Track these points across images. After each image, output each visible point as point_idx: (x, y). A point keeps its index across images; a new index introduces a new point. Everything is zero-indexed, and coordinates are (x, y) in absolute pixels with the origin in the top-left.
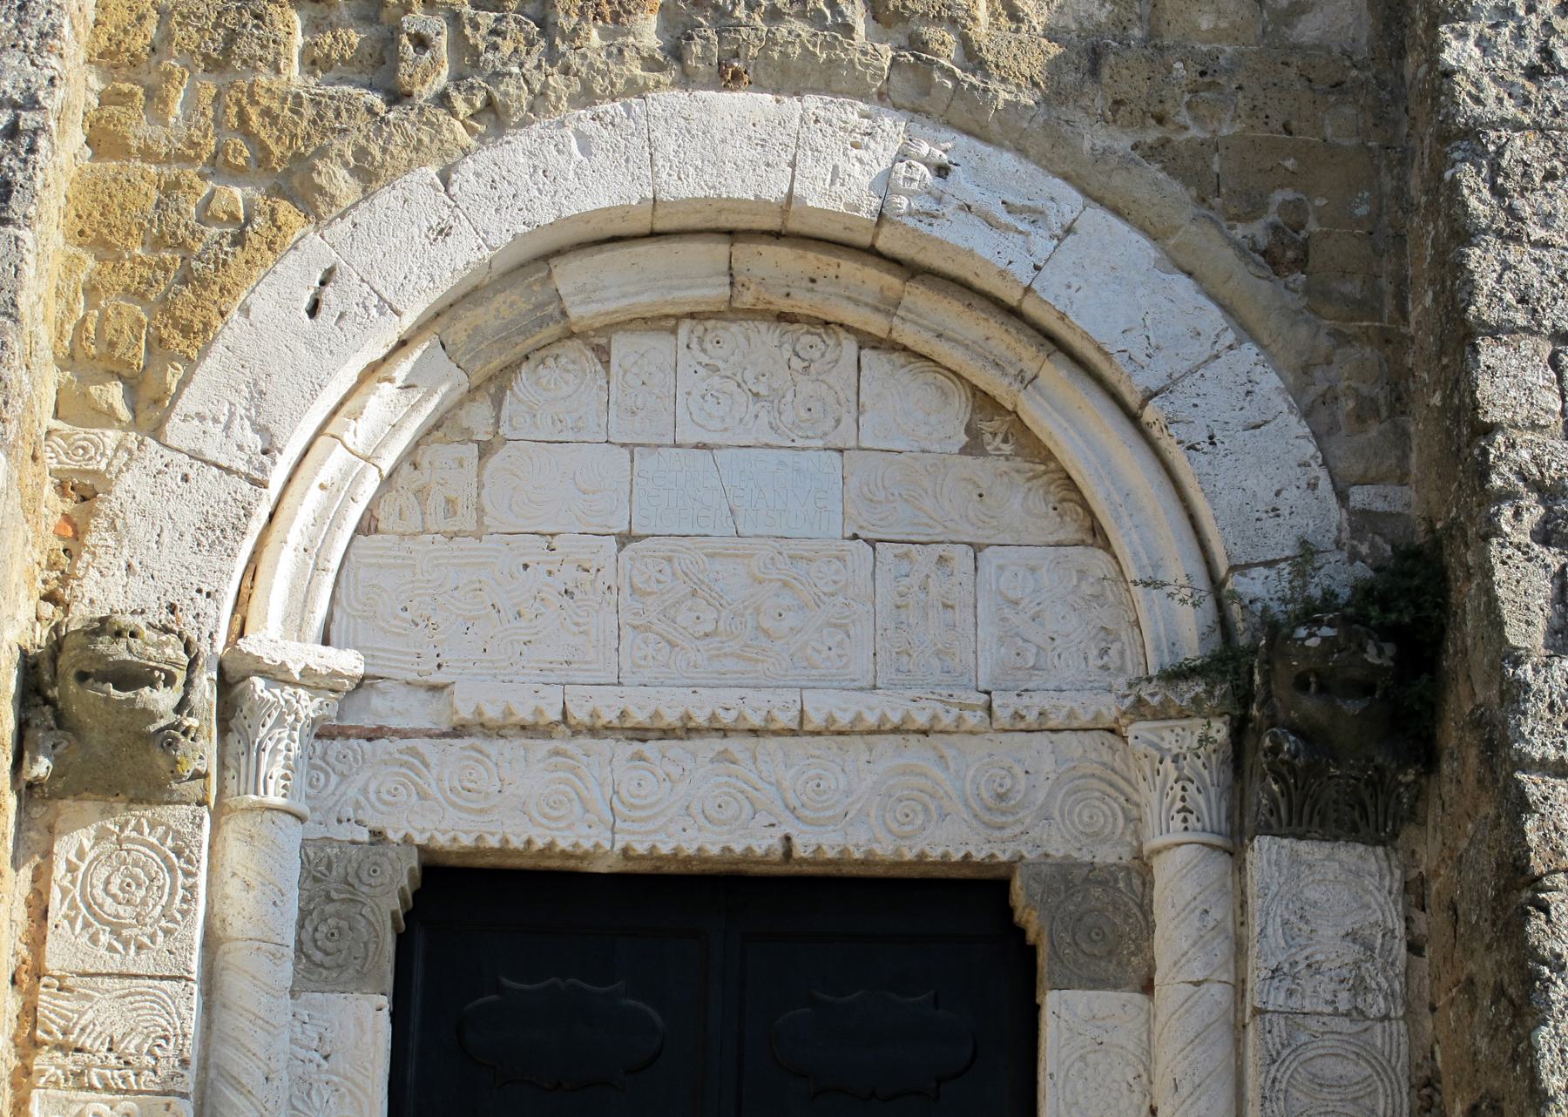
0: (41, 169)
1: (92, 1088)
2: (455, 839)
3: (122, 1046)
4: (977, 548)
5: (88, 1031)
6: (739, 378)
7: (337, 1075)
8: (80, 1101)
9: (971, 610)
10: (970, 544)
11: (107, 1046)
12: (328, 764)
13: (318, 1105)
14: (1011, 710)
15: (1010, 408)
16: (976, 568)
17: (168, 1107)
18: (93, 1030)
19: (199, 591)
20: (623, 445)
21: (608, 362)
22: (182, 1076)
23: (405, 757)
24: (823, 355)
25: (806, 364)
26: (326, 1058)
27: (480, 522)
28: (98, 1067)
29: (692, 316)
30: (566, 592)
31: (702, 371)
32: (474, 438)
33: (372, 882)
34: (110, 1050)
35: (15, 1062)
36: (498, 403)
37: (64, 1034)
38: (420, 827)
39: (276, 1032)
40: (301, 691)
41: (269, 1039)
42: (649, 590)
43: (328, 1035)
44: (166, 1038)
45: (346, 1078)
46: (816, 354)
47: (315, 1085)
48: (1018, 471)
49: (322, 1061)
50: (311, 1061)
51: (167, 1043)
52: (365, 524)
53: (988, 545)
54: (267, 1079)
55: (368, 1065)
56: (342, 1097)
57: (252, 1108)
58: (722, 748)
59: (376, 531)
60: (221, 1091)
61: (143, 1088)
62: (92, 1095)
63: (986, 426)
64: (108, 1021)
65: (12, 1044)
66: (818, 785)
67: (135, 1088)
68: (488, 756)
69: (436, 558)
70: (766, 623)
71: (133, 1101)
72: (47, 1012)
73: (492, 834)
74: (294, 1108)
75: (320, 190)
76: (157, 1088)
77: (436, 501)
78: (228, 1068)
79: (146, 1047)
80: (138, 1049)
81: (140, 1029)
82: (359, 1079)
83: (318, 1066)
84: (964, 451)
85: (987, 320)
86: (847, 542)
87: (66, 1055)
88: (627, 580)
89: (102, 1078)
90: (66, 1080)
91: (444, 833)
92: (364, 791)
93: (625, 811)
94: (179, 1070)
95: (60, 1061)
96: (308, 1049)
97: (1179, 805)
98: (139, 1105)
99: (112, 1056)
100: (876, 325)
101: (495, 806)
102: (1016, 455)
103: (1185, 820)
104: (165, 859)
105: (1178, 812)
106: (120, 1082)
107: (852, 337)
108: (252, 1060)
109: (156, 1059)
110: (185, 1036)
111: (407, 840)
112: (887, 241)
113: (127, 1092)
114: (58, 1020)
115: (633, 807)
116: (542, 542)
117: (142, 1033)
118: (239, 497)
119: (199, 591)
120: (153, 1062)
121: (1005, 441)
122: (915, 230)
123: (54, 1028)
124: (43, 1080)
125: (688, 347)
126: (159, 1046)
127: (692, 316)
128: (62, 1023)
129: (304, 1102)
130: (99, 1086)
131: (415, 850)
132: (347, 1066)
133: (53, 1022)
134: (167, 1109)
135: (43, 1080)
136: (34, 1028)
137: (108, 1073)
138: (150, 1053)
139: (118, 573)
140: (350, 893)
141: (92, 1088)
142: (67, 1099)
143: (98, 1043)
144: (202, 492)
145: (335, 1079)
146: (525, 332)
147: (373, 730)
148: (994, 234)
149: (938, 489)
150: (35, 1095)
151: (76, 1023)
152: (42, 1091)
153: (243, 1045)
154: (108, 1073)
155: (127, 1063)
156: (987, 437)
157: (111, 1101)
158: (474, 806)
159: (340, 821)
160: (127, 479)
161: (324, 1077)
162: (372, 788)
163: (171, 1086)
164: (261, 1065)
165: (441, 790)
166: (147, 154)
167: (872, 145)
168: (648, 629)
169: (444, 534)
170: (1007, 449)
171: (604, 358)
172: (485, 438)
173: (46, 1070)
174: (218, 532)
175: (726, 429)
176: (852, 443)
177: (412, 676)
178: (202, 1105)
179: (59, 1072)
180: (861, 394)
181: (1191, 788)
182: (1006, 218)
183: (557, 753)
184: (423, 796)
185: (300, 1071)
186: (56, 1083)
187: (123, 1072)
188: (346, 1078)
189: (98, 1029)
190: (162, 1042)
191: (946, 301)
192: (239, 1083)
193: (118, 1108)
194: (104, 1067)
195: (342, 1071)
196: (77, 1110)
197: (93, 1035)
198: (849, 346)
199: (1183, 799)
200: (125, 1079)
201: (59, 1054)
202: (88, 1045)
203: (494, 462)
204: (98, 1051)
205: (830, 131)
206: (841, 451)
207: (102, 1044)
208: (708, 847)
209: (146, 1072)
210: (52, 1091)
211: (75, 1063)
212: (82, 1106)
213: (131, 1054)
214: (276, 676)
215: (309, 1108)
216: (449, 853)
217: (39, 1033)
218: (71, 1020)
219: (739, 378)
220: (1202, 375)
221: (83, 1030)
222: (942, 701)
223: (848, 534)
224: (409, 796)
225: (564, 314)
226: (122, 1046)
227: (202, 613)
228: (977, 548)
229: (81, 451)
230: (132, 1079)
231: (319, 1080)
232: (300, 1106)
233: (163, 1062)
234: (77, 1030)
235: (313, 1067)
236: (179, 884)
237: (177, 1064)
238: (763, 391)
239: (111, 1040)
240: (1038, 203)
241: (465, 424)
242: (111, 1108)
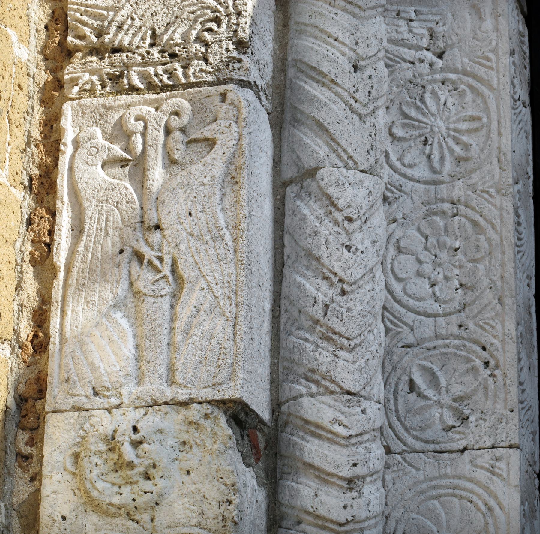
1: (133, 89)
3: (166, 37)
5: (126, 27)
7: (455, 71)
8: (119, 106)
11: (148, 41)
13: (434, 109)
17: (224, 96)
18: (131, 25)
22: (240, 61)
26: (440, 56)
28: (139, 65)
34: (152, 45)
35: (44, 77)
37: (99, 35)
39: (362, 14)
41: (355, 22)
43: (439, 29)
44: (217, 21)
45: (465, 73)
47: (429, 87)
49: (435, 59)
50: (422, 61)
51: (219, 26)
54: (356, 68)
55: (491, 55)
56: (462, 94)
57: (337, 99)
60: (300, 87)
61: (193, 80)
62: (134, 97)
64: (148, 14)
65: (41, 57)
67: (184, 81)
71: (182, 96)
72: (78, 15)
74: (406, 116)
76: (210, 78)
78: (306, 60)
79: (194, 33)
80: (185, 38)
81: (186, 15)
82: (481, 72)
83: (431, 65)
87: (102, 59)
89: (144, 77)
90: (103, 86)
94: (235, 54)
95: (94, 65)
96: (419, 48)
98: (190, 101)
99: (155, 51)
106: (165, 78)
108: (333, 46)
109: (207, 45)
110: (239, 14)
113: (173, 87)
114: (91, 21)
117: (188, 19)
120: (203, 50)
123: (87, 30)
124: (76, 89)
126: (210, 30)
128: (96, 23)
129: (417, 108)
130: (141, 86)
132: (466, 60)
133: (86, 24)
134: (223, 101)
135: (76, 89)
136: (65, 36)
137: (151, 70)
138: (198, 39)
141: (133, 89)
142: (104, 106)
143: (138, 39)
145: (453, 76)
150: (68, 108)
151: (112, 21)
152: (75, 102)
153: (322, 31)
154: (151, 70)
155: (173, 56)
157: (156, 100)
161: (439, 77)
163: (226, 73)
164: (347, 51)
173: (77, 79)
178: (283, 111)
179: (95, 78)
185: (409, 74)
186: (92, 91)
187: (168, 66)
188: (465, 73)
189: (137, 23)
190: (214, 26)
192: (320, 73)
193: (164, 107)
194: (145, 64)
195: (460, 66)
196: (117, 116)
197: (131, 32)
200: (171, 74)
201: (94, 58)
202: (126, 43)
204: (138, 47)
207: (143, 39)
209: (196, 62)
210: (87, 101)
211: (112, 65)
212: (122, 111)
213: (177, 45)
215: (424, 114)
217: (70, 39)
218: (106, 18)
221: (120, 28)
226: (166, 37)
230: (180, 72)
231: (434, 81)
232: (413, 113)
233: (215, 47)
234: (113, 29)
235: (424, 68)
237: (231, 47)
239: (154, 35)
242: (157, 109)
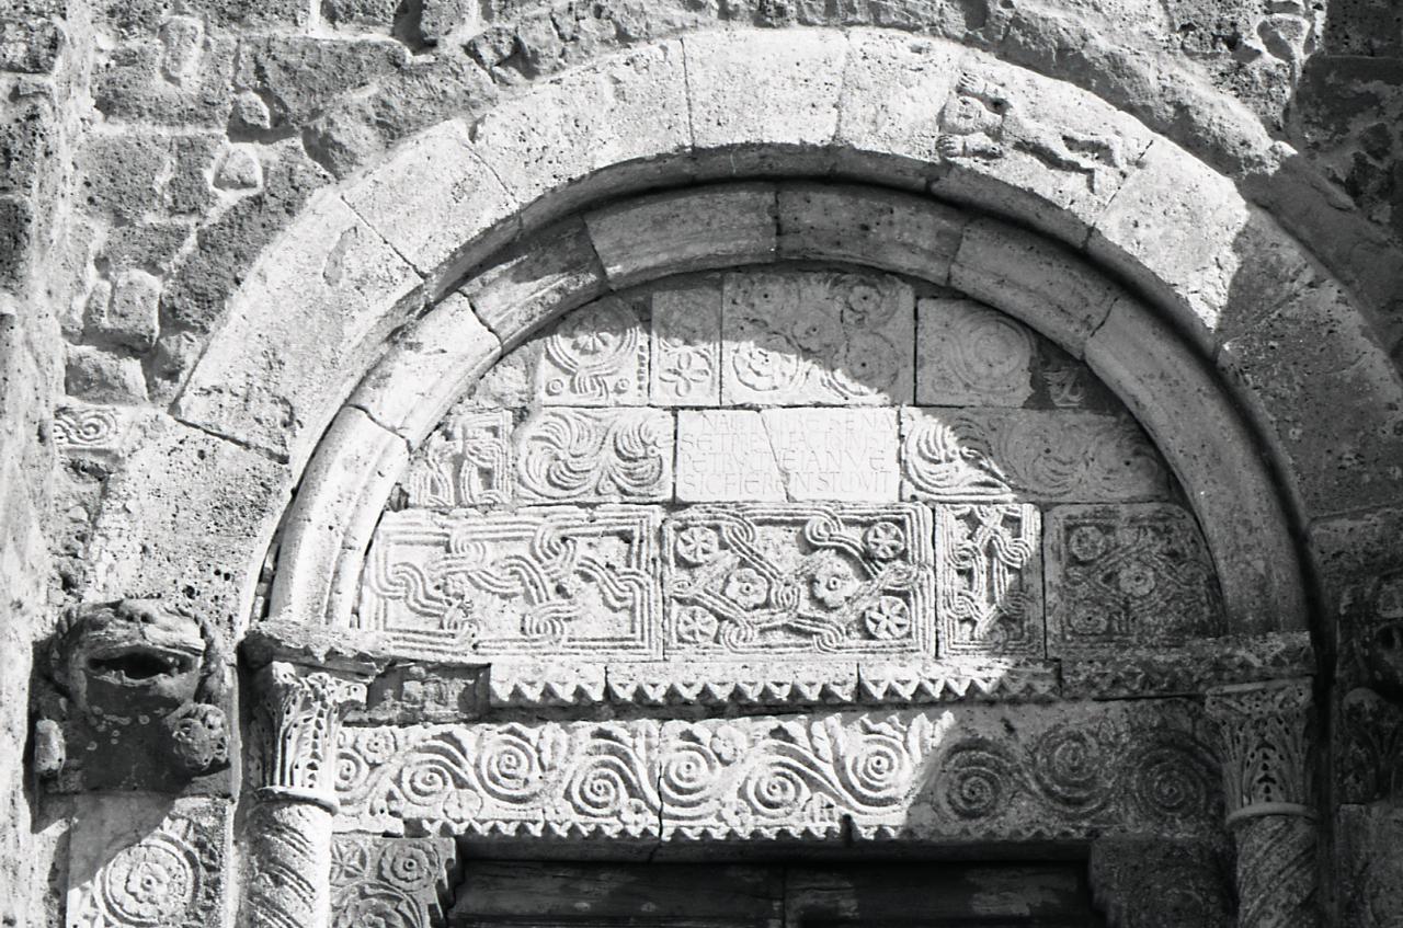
0: (41, 135)
2: (494, 829)
6: (788, 333)
9: (1039, 574)
12: (358, 752)
15: (1078, 356)
19: (218, 573)
21: (649, 320)
23: (440, 743)
24: (878, 306)
25: (859, 316)
29: (737, 269)
30: (608, 566)
33: (408, 875)
38: (458, 817)
40: (325, 675)
42: (694, 561)
46: (870, 306)
48: (1087, 424)
52: (395, 498)
53: (1058, 504)
58: (775, 727)
59: (406, 506)
63: (1051, 377)
66: (879, 763)
68: (528, 740)
69: (472, 532)
70: (821, 592)
73: (535, 823)
75: (340, 146)
77: (470, 472)
85: (1050, 264)
88: (672, 552)
91: (483, 822)
92: (398, 781)
93: (674, 795)
97: (1261, 774)
100: (936, 271)
101: (535, 794)
103: (1267, 790)
104: (188, 854)
105: (1260, 781)
107: (908, 287)
111: (445, 830)
112: (949, 185)
115: (680, 791)
116: (583, 513)
118: (257, 473)
119: (218, 573)
121: (1073, 392)
122: (971, 170)
127: (737, 269)
131: (453, 841)
139: (132, 556)
140: (386, 888)
144: (218, 469)
148: (1058, 173)
149: (1002, 444)
156: (1053, 390)
158: (516, 793)
159: (372, 812)
160: (142, 457)
165: (480, 778)
166: (159, 114)
167: (925, 81)
168: (694, 602)
170: (1075, 399)
174: (236, 511)
175: (775, 388)
181: (1274, 756)
182: (1065, 154)
183: (602, 734)
191: (1006, 246)
198: (906, 296)
199: (1265, 767)
205: (878, 68)
208: (765, 831)
214: (305, 662)
216: (488, 845)
220: (1280, 315)
224: (445, 783)
227: (221, 595)
229: (92, 429)
236: (202, 881)
238: (815, 347)
240: (1102, 139)
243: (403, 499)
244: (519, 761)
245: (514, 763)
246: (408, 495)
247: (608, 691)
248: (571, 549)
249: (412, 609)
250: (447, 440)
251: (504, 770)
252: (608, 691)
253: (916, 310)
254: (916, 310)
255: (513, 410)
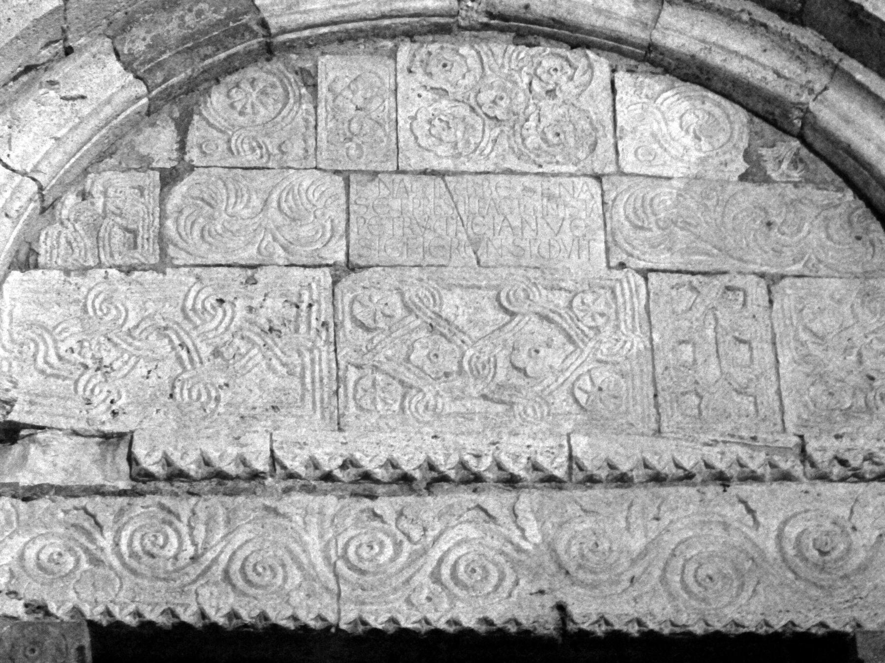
4: (771, 281)
6: (472, 101)
10: (762, 275)
14: (830, 454)
16: (771, 302)
20: (337, 172)
27: (163, 252)
31: (430, 95)
32: (154, 165)
36: (183, 128)
42: (373, 325)
52: (22, 257)
59: (36, 266)
70: (522, 359)
84: (743, 178)
86: (615, 272)
102: (808, 181)
125: (410, 71)
146: (218, 44)
147: (31, 488)
156: (769, 166)
162: (31, 554)
169: (119, 268)
170: (796, 175)
171: (310, 81)
172: (168, 166)
176: (611, 169)
177: (81, 426)
180: (619, 119)
184: (96, 561)
203: (180, 190)
206: (598, 178)
219: (472, 101)
222: (745, 445)
223: (613, 263)
225: (264, 24)
228: (771, 281)
241: (143, 150)
243: (32, 260)
244: (167, 538)
245: (161, 541)
246: (38, 254)
247: (274, 460)
248: (229, 313)
249: (42, 372)
250: (84, 199)
251: (149, 546)
252: (274, 460)
253: (613, 83)
254: (613, 83)
255: (162, 170)
